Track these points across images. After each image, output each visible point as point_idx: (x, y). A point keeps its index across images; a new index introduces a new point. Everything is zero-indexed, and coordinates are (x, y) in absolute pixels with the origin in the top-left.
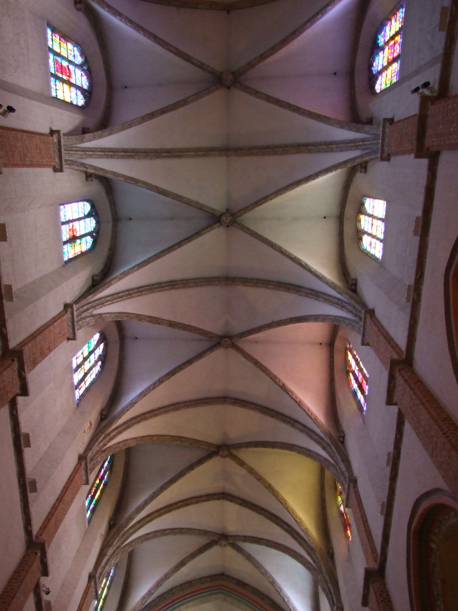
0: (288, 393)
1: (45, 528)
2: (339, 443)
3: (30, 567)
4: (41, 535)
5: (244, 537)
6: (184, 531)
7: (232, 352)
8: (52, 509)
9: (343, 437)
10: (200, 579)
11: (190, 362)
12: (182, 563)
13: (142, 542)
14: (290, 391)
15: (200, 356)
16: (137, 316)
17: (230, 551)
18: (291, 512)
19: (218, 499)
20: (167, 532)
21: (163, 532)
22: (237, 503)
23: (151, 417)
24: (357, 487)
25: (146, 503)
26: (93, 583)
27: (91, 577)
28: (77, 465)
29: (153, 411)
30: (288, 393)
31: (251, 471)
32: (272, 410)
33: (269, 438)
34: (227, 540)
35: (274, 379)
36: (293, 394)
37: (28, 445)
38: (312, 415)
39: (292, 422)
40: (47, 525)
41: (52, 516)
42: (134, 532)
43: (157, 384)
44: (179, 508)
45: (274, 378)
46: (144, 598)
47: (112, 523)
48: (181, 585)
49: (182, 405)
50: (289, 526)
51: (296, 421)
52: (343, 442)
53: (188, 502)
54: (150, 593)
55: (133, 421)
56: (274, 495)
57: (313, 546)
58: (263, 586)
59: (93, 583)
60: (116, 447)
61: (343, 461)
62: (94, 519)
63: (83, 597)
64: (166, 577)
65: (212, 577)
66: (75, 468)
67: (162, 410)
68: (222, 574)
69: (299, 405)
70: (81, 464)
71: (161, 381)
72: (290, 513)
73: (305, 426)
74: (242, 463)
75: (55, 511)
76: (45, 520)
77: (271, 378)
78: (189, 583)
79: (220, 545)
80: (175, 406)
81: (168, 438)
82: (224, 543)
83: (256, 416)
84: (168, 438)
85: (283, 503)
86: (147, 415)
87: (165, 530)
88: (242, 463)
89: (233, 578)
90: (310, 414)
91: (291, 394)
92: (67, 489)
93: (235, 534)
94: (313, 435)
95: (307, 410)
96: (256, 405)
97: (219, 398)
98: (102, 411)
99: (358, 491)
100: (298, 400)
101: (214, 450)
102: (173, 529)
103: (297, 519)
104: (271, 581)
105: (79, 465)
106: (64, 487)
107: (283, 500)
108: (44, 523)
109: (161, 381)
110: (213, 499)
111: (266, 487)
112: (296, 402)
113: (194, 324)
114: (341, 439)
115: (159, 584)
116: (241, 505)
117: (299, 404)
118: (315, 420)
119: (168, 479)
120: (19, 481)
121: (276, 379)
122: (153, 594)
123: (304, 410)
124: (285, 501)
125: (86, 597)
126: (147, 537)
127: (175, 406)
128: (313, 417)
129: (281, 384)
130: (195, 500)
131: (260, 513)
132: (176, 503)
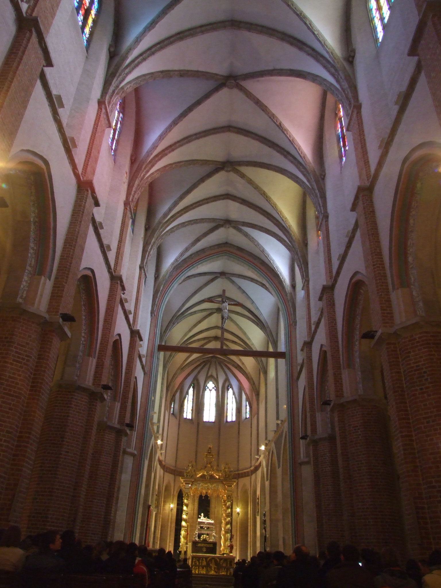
0: (283, 132)
1: (117, 263)
2: (320, 179)
3: (117, 292)
4: (116, 269)
5: (243, 222)
6: (198, 221)
7: (236, 91)
8: (117, 249)
9: (324, 176)
10: (210, 247)
11: (198, 103)
12: (198, 240)
13: (169, 235)
14: (285, 130)
15: (207, 96)
16: (152, 76)
17: (232, 231)
18: (280, 214)
19: (223, 199)
20: (186, 224)
21: (183, 225)
22: (238, 202)
23: (170, 152)
24: (328, 221)
25: (170, 210)
26: (143, 271)
27: (141, 268)
28: (124, 210)
29: (170, 146)
30: (283, 132)
31: (250, 182)
32: (269, 141)
33: (266, 161)
34: (230, 224)
35: (273, 118)
36: (287, 133)
37: (102, 228)
38: (301, 153)
39: (285, 153)
40: (118, 262)
41: (119, 254)
42: (164, 230)
43: (172, 126)
44: (194, 208)
45: (272, 117)
46: (173, 264)
47: (147, 227)
48: (197, 252)
49: (194, 137)
50: (277, 221)
51: (288, 153)
52: (323, 178)
53: (201, 203)
54: (176, 260)
55: (156, 159)
56: (267, 200)
57: (294, 238)
58: (256, 251)
59: (143, 271)
60: (147, 182)
61: (321, 197)
62: (135, 229)
63: (138, 281)
64: (187, 249)
65: (219, 245)
66: (124, 213)
67: (177, 145)
68: (226, 243)
69: (292, 144)
70: (127, 209)
71: (175, 123)
72: (278, 214)
73: (295, 158)
74: (243, 176)
75: (120, 250)
76: (116, 258)
77: (270, 118)
78: (203, 250)
79: (225, 227)
80: (187, 140)
81: (184, 163)
82: (227, 226)
83: (256, 144)
84: (184, 163)
85: (274, 206)
86: (166, 152)
87: (184, 223)
88: (243, 176)
89: (234, 246)
90: (300, 153)
91: (286, 133)
92: (123, 232)
93: (237, 220)
94: (301, 167)
95: (298, 149)
96: (256, 135)
97: (223, 127)
98: (132, 156)
99: (328, 225)
100: (291, 139)
101: (220, 166)
102: (190, 221)
103: (284, 219)
104: (262, 250)
105: (126, 210)
106: (121, 231)
107: (274, 204)
108: (115, 261)
109: (175, 123)
110: (220, 200)
111: (261, 194)
112: (290, 140)
113: (201, 69)
114: (322, 177)
115: (182, 254)
116: (241, 203)
117: (292, 142)
118: (303, 158)
119: (185, 189)
120: (101, 249)
121: (274, 118)
122: (179, 261)
123: (296, 148)
124: (275, 205)
125: (140, 280)
126: (172, 230)
127: (187, 140)
128: (302, 155)
129: (278, 124)
130: (205, 201)
131: (256, 210)
132: (191, 205)
